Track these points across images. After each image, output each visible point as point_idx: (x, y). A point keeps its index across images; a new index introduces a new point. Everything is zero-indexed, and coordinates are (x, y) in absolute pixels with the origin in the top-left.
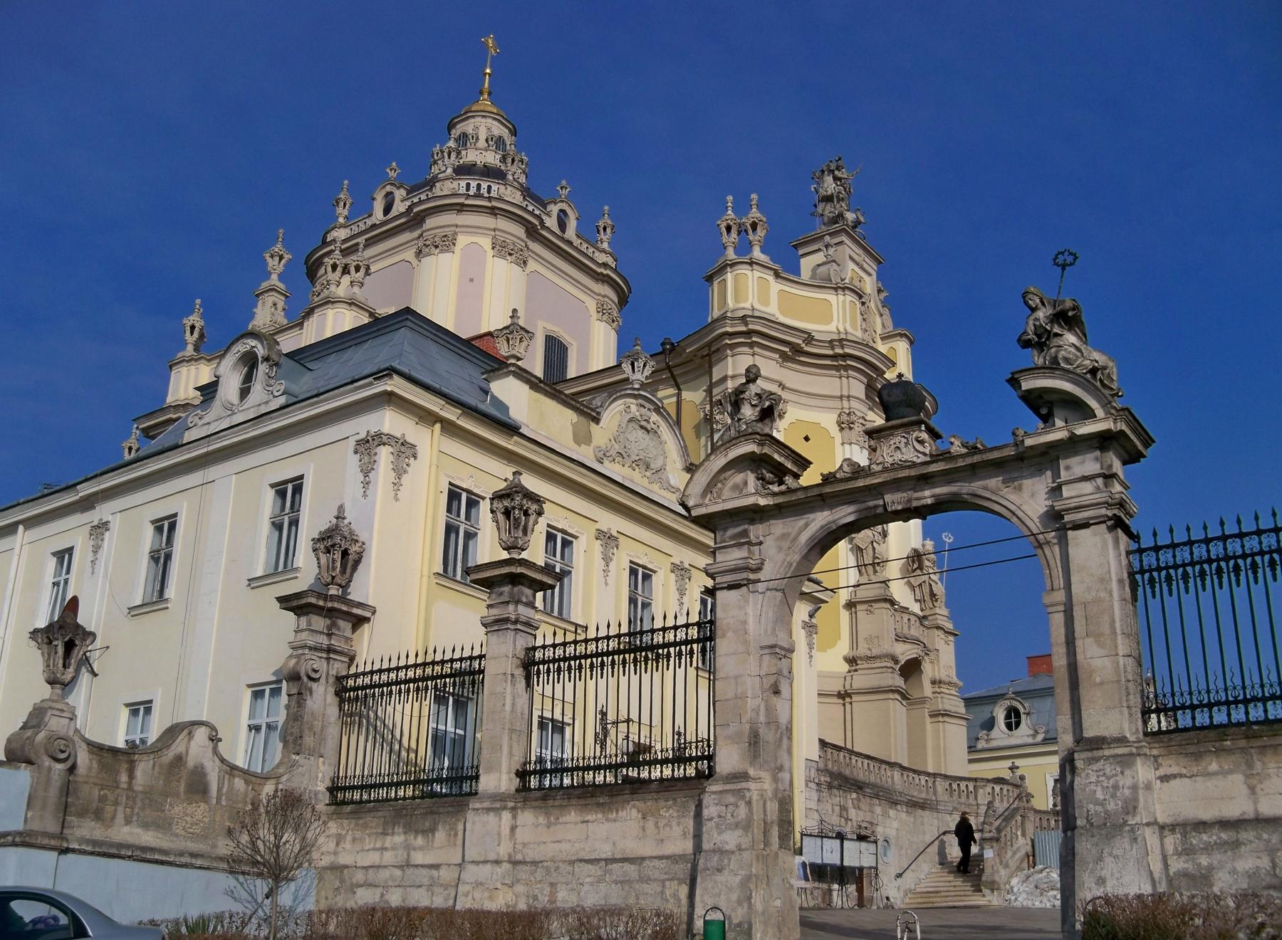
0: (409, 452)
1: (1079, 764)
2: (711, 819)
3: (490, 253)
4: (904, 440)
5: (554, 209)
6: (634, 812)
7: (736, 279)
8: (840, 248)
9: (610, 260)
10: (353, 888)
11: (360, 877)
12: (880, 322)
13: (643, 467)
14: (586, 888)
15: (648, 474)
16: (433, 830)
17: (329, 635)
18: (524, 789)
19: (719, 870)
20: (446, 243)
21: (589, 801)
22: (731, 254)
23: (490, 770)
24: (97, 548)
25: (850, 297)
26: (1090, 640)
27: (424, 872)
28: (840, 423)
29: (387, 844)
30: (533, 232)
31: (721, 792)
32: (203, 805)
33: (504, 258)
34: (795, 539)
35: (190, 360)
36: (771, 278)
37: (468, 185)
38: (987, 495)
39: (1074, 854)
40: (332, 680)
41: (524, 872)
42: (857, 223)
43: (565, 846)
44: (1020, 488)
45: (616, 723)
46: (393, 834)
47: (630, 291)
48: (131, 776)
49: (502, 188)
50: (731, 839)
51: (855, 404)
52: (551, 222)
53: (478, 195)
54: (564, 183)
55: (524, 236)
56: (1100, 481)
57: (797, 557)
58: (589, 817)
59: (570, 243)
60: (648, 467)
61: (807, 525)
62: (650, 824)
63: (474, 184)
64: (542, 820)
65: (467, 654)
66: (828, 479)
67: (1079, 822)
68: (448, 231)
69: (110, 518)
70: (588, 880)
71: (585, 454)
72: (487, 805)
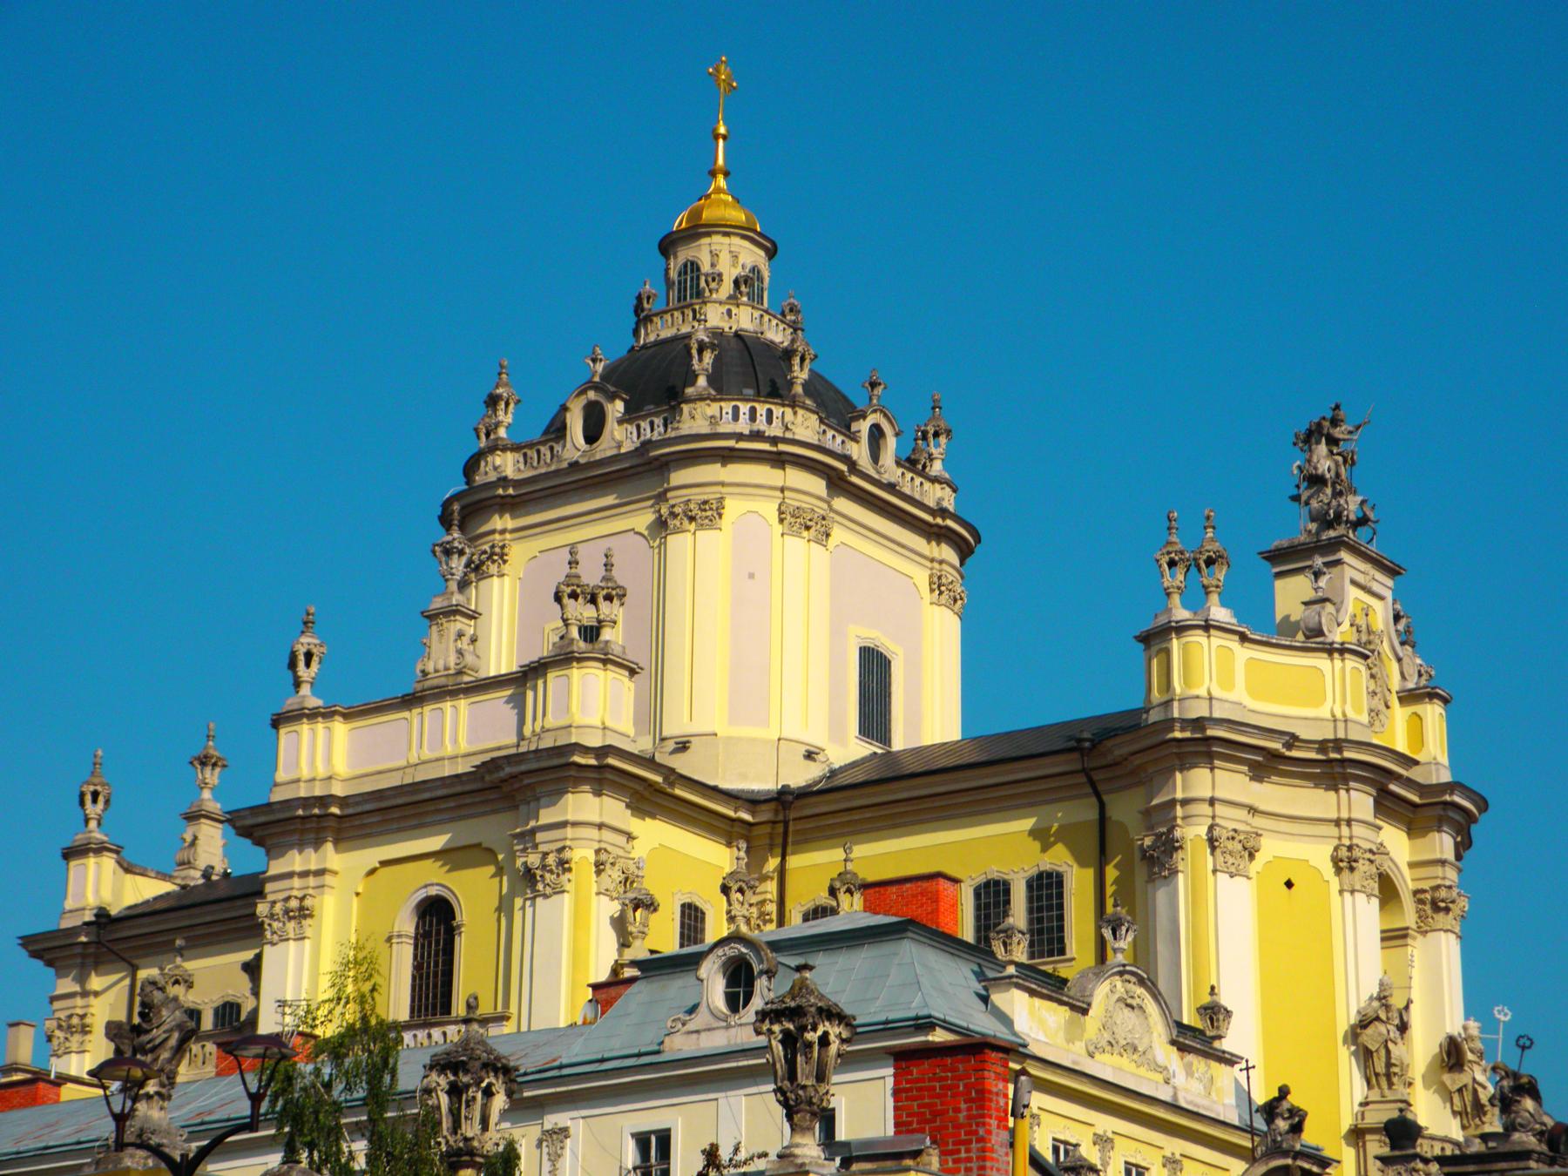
3: (778, 529)
5: (863, 427)
7: (1185, 649)
8: (1335, 570)
9: (948, 500)
13: (1130, 1051)
15: (1135, 1057)
20: (707, 513)
24: (555, 1158)
28: (1336, 861)
30: (837, 484)
33: (799, 535)
35: (313, 715)
36: (1233, 643)
37: (736, 409)
47: (978, 540)
49: (788, 411)
51: (1358, 830)
52: (859, 451)
53: (757, 436)
55: (823, 492)
59: (891, 487)
60: (1135, 1049)
68: (709, 494)
69: (569, 1123)
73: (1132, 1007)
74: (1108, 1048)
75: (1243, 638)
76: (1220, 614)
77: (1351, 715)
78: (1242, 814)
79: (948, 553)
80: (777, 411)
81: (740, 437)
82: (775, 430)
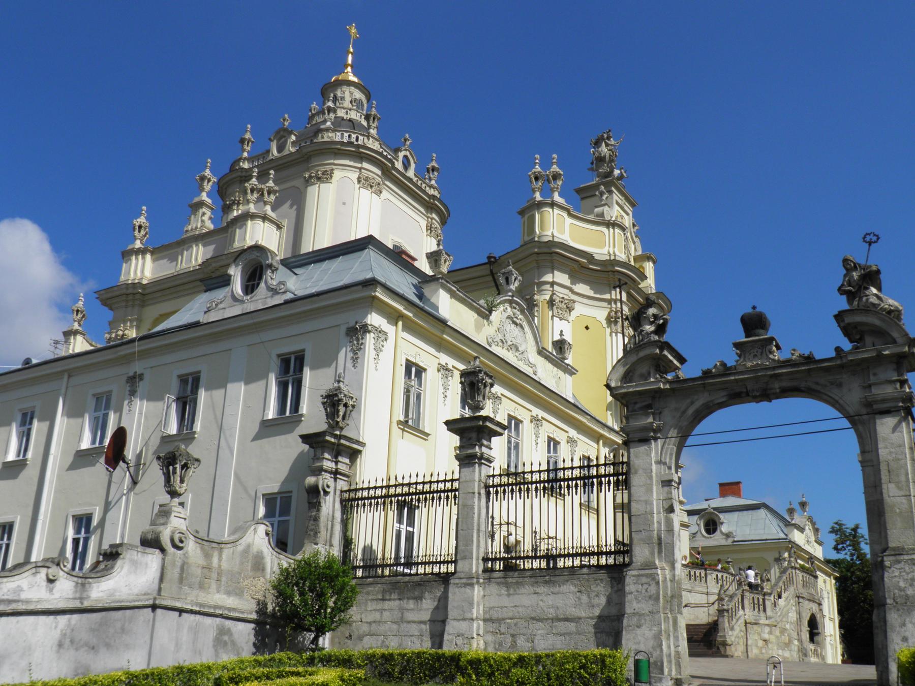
0: (383, 337)
1: (887, 563)
2: (632, 593)
4: (760, 351)
5: (401, 155)
6: (572, 588)
9: (436, 193)
10: (360, 638)
11: (365, 628)
12: (636, 249)
14: (538, 637)
16: (419, 598)
17: (336, 463)
18: (485, 570)
19: (638, 627)
20: (326, 177)
21: (540, 579)
22: (538, 197)
23: (464, 558)
25: (617, 231)
26: (892, 486)
27: (414, 625)
29: (386, 607)
31: (639, 576)
32: (262, 579)
34: (684, 412)
35: (138, 252)
36: (565, 214)
37: (342, 135)
38: (818, 388)
39: (885, 622)
40: (338, 493)
41: (492, 627)
42: (621, 177)
43: (520, 609)
44: (840, 385)
45: (501, 524)
46: (390, 600)
47: (449, 215)
48: (220, 560)
50: (644, 607)
52: (399, 165)
54: (407, 136)
56: (898, 385)
57: (685, 423)
58: (538, 590)
59: (410, 180)
60: (517, 350)
61: (692, 403)
62: (584, 598)
63: (346, 135)
64: (504, 591)
65: (442, 478)
66: (707, 374)
67: (889, 601)
68: (328, 168)
70: (539, 632)
71: (481, 339)
72: (464, 581)
73: (514, 323)
74: (500, 344)
75: (570, 215)
76: (557, 197)
77: (617, 253)
78: (567, 292)
79: (434, 216)
80: (361, 138)
81: (342, 143)
82: (360, 142)
